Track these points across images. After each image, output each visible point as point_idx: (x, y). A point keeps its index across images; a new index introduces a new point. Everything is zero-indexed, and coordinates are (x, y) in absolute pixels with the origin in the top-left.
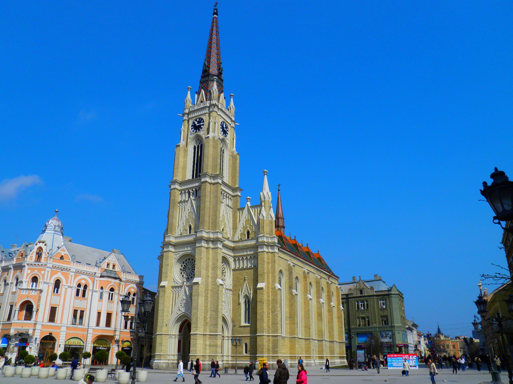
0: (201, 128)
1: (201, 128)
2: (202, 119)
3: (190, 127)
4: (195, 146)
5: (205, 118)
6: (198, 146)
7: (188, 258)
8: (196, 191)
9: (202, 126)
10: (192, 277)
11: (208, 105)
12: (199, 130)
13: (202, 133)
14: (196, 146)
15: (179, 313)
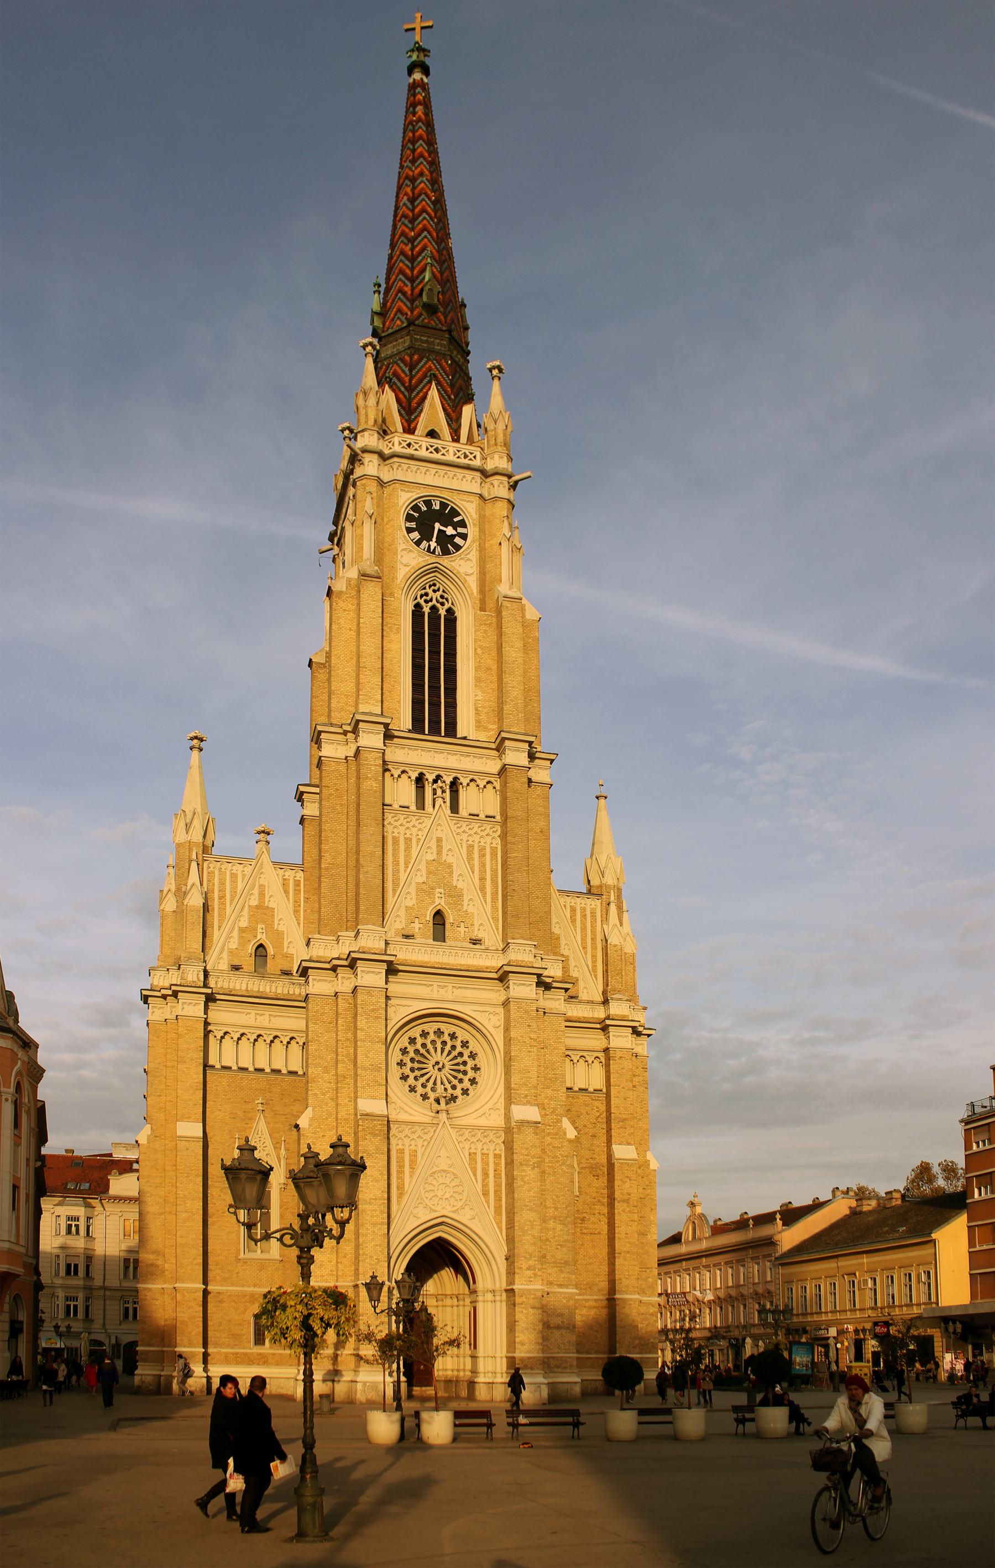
0: (458, 548)
1: (458, 548)
2: (455, 513)
3: (402, 523)
4: (418, 606)
5: (469, 510)
6: (434, 608)
7: (435, 1026)
8: (454, 784)
9: (458, 540)
10: (454, 1098)
11: (477, 463)
12: (446, 552)
13: (464, 564)
14: (426, 610)
15: (424, 1216)
